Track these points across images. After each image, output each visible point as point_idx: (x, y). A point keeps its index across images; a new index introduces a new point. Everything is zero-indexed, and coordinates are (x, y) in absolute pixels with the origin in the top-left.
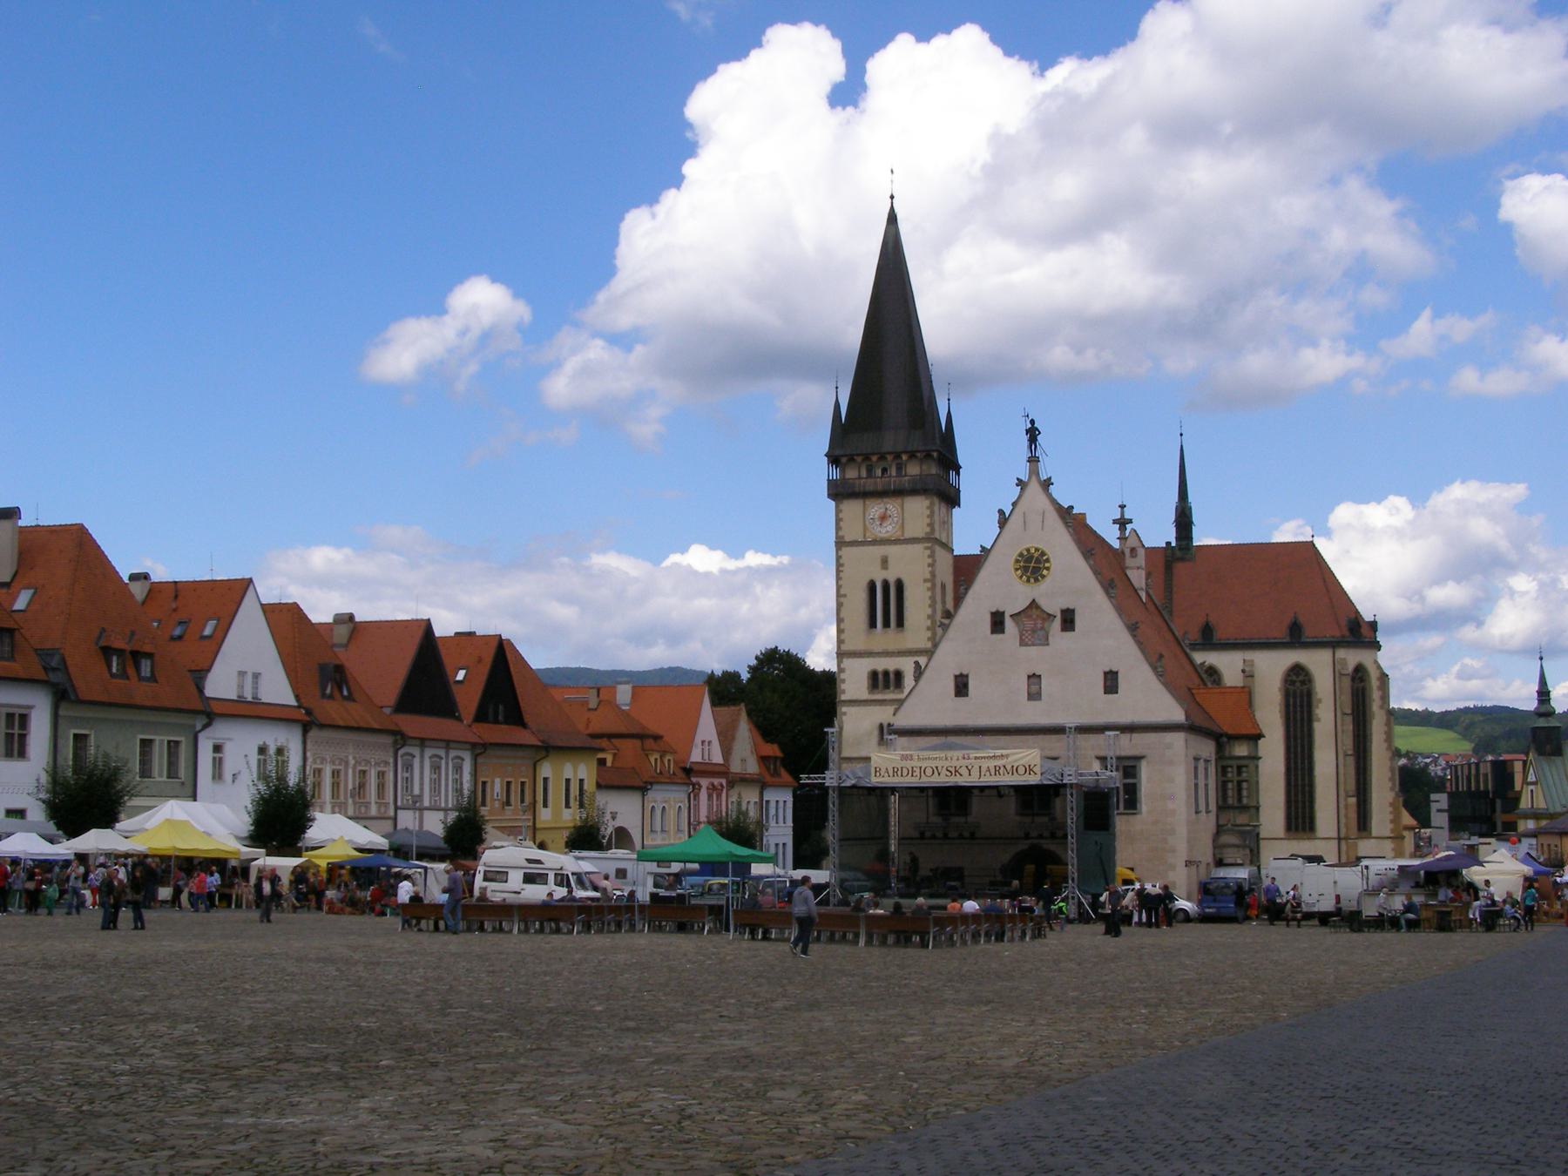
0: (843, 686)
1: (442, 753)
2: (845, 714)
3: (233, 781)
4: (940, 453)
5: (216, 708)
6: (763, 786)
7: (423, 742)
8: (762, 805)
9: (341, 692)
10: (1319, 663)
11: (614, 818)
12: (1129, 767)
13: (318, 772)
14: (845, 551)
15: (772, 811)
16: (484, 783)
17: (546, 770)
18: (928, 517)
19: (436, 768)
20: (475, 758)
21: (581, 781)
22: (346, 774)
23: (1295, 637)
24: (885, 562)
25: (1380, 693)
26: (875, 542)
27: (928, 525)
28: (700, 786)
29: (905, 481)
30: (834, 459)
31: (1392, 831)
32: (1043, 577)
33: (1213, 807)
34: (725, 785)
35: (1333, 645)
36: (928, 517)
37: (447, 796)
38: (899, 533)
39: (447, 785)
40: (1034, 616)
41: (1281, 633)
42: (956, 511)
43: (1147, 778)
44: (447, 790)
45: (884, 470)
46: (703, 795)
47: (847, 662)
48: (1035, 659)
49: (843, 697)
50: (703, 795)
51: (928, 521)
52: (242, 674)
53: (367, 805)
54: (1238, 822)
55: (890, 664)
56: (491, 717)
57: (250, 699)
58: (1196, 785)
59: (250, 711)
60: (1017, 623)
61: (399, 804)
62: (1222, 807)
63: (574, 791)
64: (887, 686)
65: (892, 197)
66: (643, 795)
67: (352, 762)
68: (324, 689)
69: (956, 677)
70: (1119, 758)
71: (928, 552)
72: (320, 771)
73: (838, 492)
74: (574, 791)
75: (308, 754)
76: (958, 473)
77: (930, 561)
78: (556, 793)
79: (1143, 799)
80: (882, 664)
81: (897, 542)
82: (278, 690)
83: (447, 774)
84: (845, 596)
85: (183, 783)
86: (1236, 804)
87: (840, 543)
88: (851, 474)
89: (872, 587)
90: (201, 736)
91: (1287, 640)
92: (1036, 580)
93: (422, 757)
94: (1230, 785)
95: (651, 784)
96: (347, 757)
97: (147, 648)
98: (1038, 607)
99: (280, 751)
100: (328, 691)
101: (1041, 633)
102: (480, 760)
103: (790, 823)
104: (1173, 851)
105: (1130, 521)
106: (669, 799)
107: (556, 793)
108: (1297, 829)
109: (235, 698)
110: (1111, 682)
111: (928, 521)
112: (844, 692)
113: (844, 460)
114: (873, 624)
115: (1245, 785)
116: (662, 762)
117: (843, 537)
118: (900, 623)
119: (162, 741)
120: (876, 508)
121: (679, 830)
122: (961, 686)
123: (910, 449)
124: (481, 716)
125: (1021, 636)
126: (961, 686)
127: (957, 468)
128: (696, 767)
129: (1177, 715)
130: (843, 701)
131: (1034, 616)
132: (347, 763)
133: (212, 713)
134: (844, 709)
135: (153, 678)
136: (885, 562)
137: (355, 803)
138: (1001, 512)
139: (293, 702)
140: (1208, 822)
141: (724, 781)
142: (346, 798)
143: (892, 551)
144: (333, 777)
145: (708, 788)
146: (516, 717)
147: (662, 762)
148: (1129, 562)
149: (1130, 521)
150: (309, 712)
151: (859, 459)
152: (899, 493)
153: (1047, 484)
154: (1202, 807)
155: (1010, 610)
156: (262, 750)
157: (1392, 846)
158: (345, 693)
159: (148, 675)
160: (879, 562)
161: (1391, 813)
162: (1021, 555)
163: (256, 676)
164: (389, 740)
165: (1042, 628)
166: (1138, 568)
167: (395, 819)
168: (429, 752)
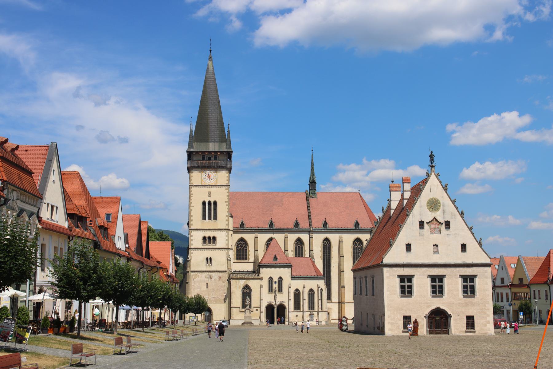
0: (192, 242)
2: (192, 253)
14: (193, 189)
18: (227, 177)
24: (209, 194)
26: (205, 186)
27: (227, 180)
36: (227, 177)
40: (435, 223)
41: (352, 226)
48: (436, 239)
51: (227, 178)
60: (429, 226)
64: (209, 242)
69: (406, 245)
71: (227, 191)
79: (477, 291)
81: (215, 186)
84: (193, 206)
89: (204, 203)
91: (354, 228)
98: (436, 220)
104: (489, 310)
110: (464, 248)
111: (227, 178)
112: (192, 245)
114: (204, 218)
118: (215, 218)
122: (408, 247)
123: (221, 150)
125: (430, 230)
126: (408, 247)
130: (192, 249)
131: (435, 223)
134: (192, 251)
136: (209, 194)
143: (212, 189)
151: (201, 153)
155: (426, 220)
160: (207, 194)
163: (121, 237)
165: (438, 228)
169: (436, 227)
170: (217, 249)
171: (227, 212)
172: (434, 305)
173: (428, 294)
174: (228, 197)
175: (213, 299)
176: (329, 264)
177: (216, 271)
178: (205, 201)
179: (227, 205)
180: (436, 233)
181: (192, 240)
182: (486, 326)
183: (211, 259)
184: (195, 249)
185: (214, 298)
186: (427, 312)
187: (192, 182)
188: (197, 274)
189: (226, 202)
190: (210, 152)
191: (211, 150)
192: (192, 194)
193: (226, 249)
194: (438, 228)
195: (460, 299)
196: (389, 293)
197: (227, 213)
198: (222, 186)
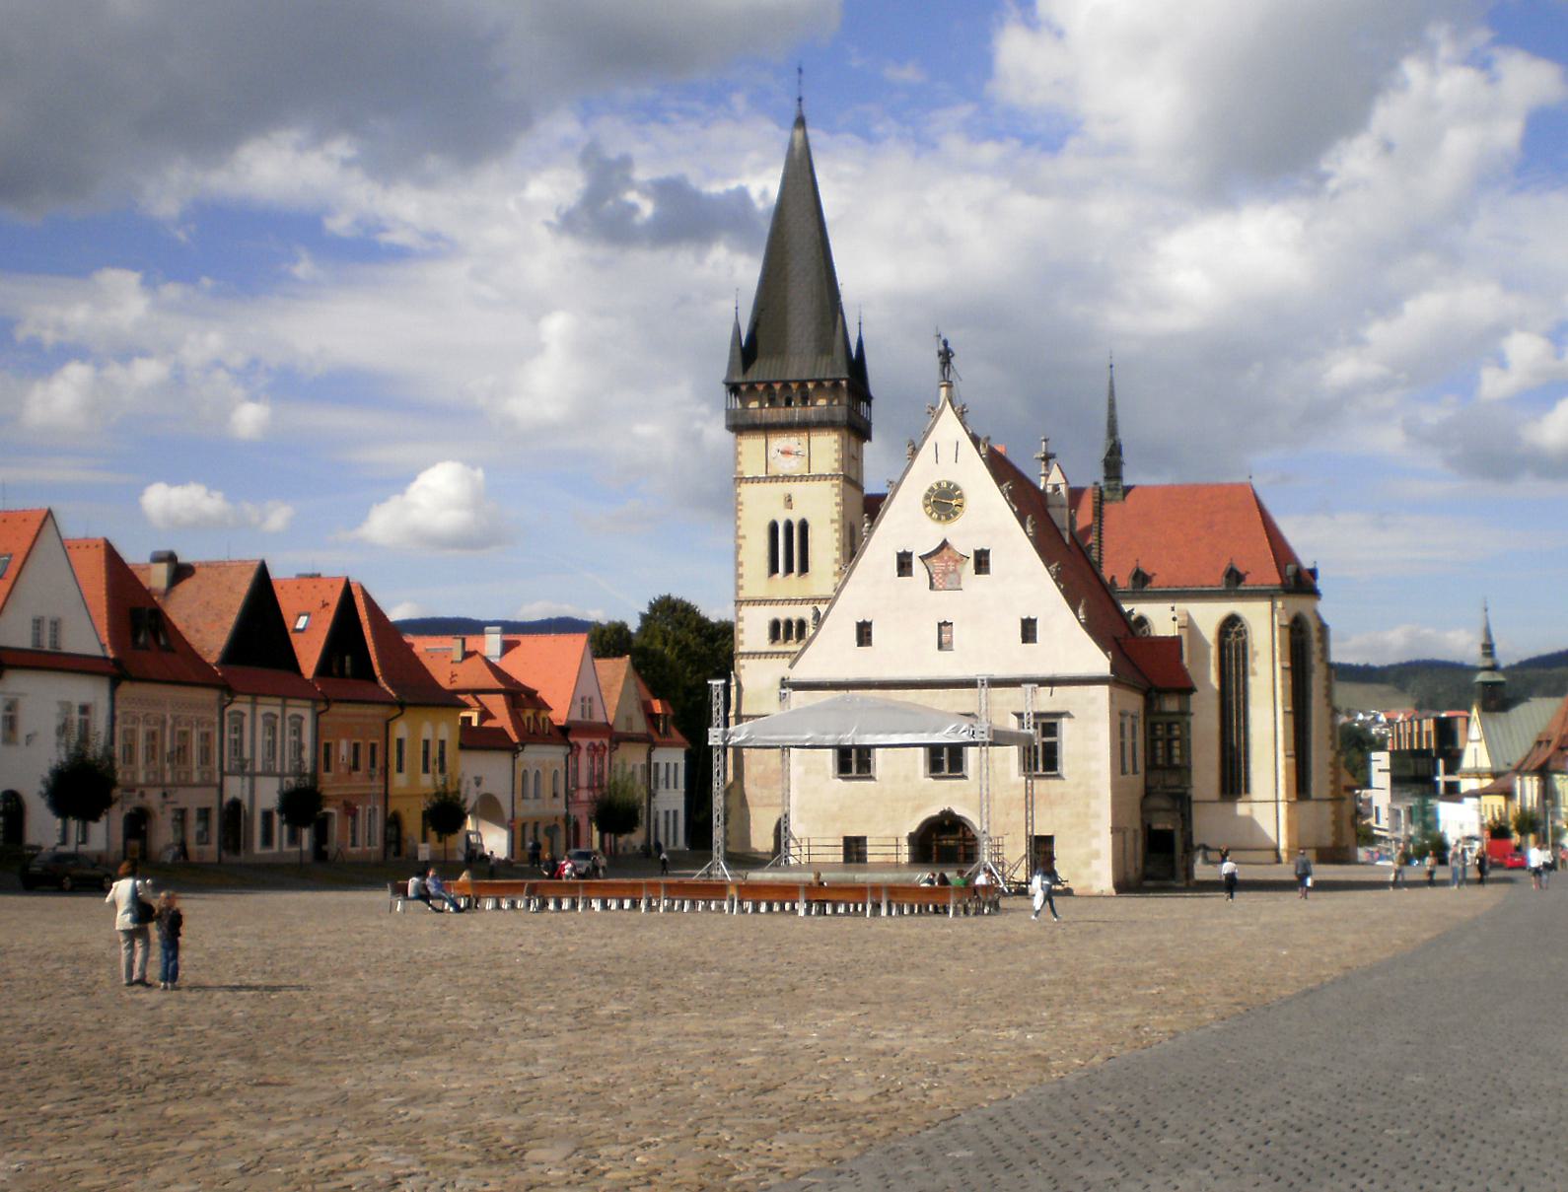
2: (743, 667)
8: (650, 769)
9: (157, 640)
11: (478, 783)
12: (1049, 724)
15: (662, 774)
16: (327, 746)
17: (400, 729)
20: (317, 716)
21: (442, 742)
26: (776, 478)
28: (579, 748)
30: (734, 389)
34: (607, 744)
42: (866, 445)
44: (283, 754)
46: (584, 759)
47: (745, 610)
48: (944, 604)
49: (741, 649)
50: (584, 759)
53: (189, 773)
55: (794, 613)
56: (335, 671)
58: (1122, 744)
61: (226, 769)
63: (434, 752)
67: (170, 722)
68: (135, 636)
70: (1037, 715)
71: (836, 490)
74: (434, 752)
76: (869, 404)
78: (413, 756)
80: (784, 613)
81: (802, 478)
83: (283, 736)
84: (744, 537)
89: (773, 528)
92: (948, 518)
95: (523, 745)
100: (142, 639)
101: (952, 576)
102: (324, 719)
103: (682, 788)
106: (545, 758)
107: (413, 756)
110: (1028, 630)
112: (742, 643)
113: (744, 388)
114: (774, 569)
116: (536, 719)
117: (742, 473)
118: (804, 568)
120: (779, 442)
121: (555, 795)
122: (864, 633)
123: (817, 377)
126: (864, 633)
129: (1099, 663)
130: (743, 654)
132: (164, 722)
134: (742, 662)
136: (789, 500)
137: (173, 768)
140: (1137, 782)
141: (606, 742)
142: (162, 761)
145: (588, 749)
147: (536, 719)
152: (804, 426)
155: (918, 551)
162: (931, 490)
166: (1062, 506)
167: (221, 788)
171: (837, 549)
179: (836, 531)
180: (949, 586)
181: (742, 631)
182: (1087, 864)
184: (749, 654)
187: (739, 469)
189: (832, 521)
190: (786, 385)
191: (792, 375)
192: (741, 504)
194: (955, 571)
196: (801, 769)
198: (822, 477)
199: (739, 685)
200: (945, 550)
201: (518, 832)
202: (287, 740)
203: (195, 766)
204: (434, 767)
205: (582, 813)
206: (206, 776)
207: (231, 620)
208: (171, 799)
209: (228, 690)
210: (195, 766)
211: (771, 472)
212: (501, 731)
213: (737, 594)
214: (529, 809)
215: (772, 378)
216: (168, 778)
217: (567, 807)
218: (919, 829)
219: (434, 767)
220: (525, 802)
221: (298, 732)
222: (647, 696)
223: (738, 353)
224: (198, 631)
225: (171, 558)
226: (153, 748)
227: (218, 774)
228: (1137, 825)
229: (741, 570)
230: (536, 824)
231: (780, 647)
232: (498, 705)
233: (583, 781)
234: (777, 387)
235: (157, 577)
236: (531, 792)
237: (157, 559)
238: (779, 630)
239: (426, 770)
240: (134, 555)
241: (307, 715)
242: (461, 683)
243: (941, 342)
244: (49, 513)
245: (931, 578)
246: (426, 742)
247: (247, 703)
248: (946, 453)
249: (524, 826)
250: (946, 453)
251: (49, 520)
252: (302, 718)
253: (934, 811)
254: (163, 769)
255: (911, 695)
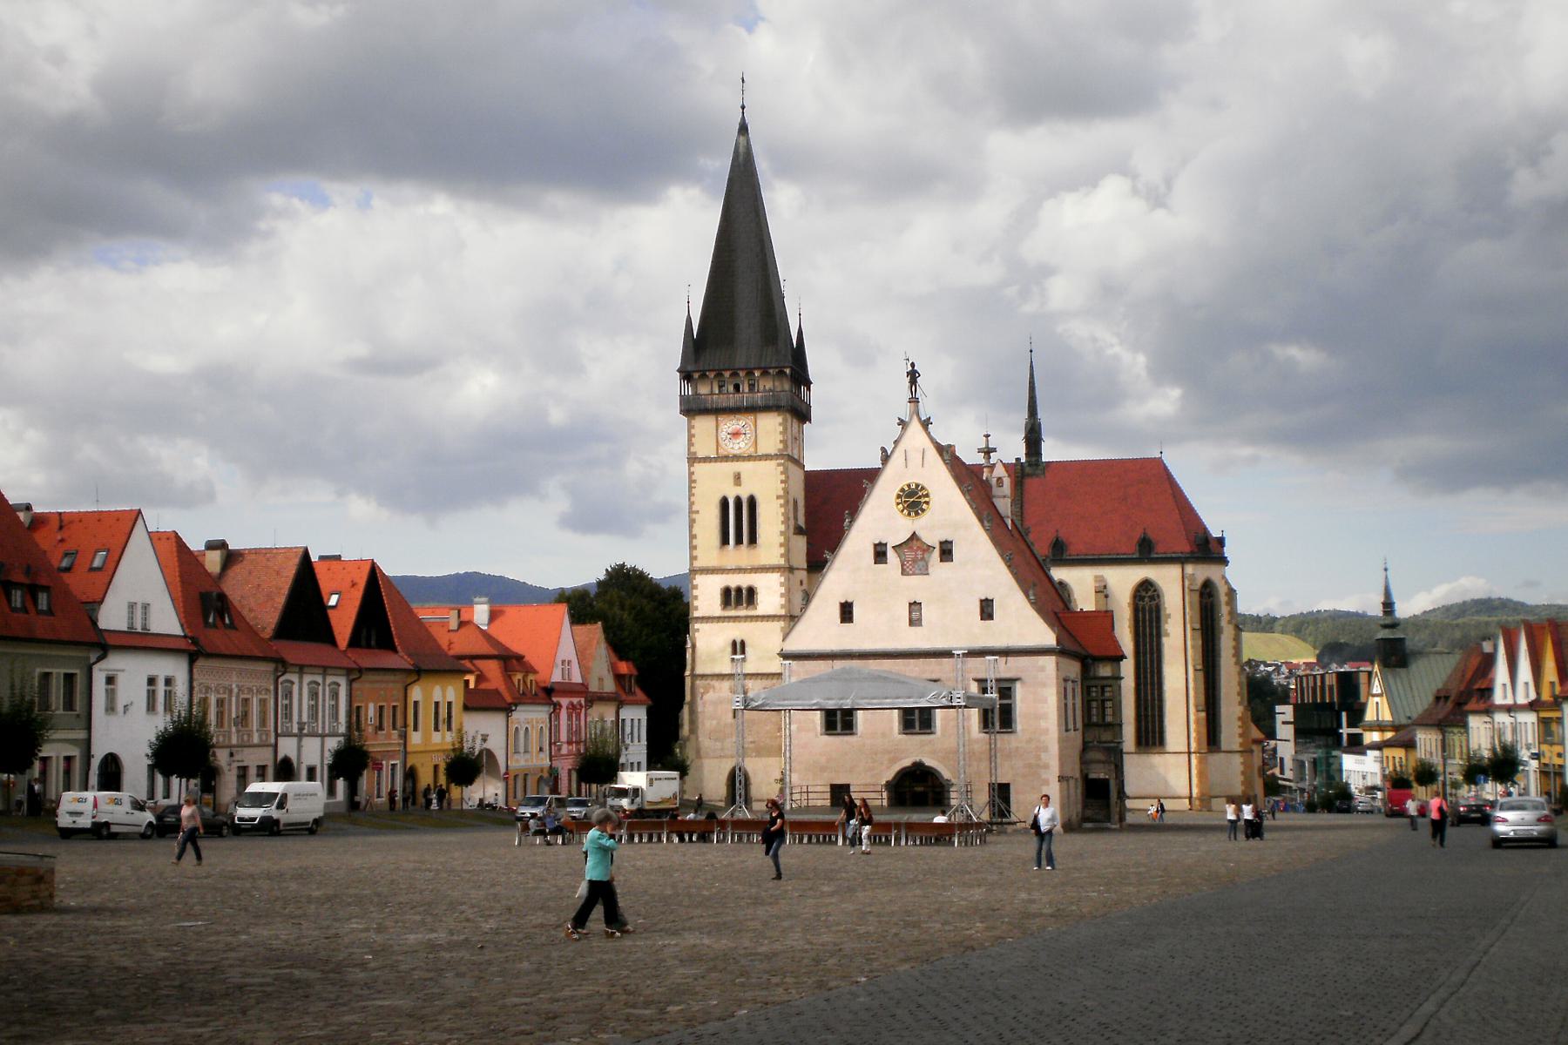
0: (696, 603)
1: (319, 679)
2: (698, 630)
3: (125, 713)
4: (792, 369)
5: (111, 641)
6: (620, 704)
7: (301, 669)
8: (618, 723)
9: (223, 620)
10: (1170, 581)
12: (1006, 688)
13: (204, 701)
14: (698, 467)
15: (628, 730)
16: (358, 708)
17: (416, 693)
18: (781, 433)
19: (314, 695)
20: (350, 683)
21: (450, 704)
22: (230, 700)
23: (1146, 553)
24: (737, 478)
25: (1229, 608)
26: (726, 458)
28: (561, 706)
29: (758, 398)
30: (686, 376)
31: (1241, 745)
32: (923, 510)
33: (1079, 725)
34: (583, 702)
35: (1181, 560)
36: (781, 433)
37: (324, 723)
38: (752, 450)
39: (324, 711)
41: (1131, 548)
42: (806, 426)
43: (1022, 699)
44: (324, 717)
45: (737, 388)
48: (915, 587)
49: (696, 614)
52: (132, 606)
53: (250, 735)
54: (1104, 739)
56: (363, 642)
57: (139, 630)
58: (1066, 705)
59: (140, 642)
61: (279, 731)
62: (1088, 725)
64: (739, 603)
65: (743, 107)
66: (508, 717)
67: (235, 690)
68: (206, 618)
70: (998, 680)
71: (781, 468)
72: (246, 701)
73: (692, 408)
75: (195, 684)
76: (809, 389)
77: (783, 477)
78: (427, 717)
79: (1018, 720)
80: (734, 581)
81: (749, 458)
82: (166, 620)
83: (324, 700)
84: (698, 512)
85: (78, 716)
86: (1100, 722)
87: (693, 459)
88: (704, 389)
89: (724, 503)
90: (96, 668)
92: (917, 514)
93: (301, 683)
94: (1094, 704)
95: (516, 705)
96: (231, 685)
97: (44, 582)
98: (918, 539)
99: (168, 681)
100: (211, 620)
101: (921, 563)
102: (355, 685)
103: (644, 742)
104: (1046, 767)
105: (994, 450)
106: (532, 717)
107: (427, 717)
108: (1147, 744)
109: (126, 629)
110: (987, 610)
112: (696, 609)
113: (696, 376)
114: (725, 541)
115: (1109, 704)
116: (525, 682)
117: (695, 453)
118: (753, 540)
119: (58, 674)
120: (729, 424)
121: (541, 749)
122: (846, 612)
123: (763, 365)
124: (355, 642)
126: (846, 612)
127: (808, 383)
128: (556, 687)
129: (1048, 637)
130: (697, 618)
132: (231, 691)
133: (105, 644)
134: (697, 626)
135: (50, 612)
136: (737, 478)
137: (238, 731)
138: (884, 450)
139: (178, 631)
140: (1076, 738)
141: (583, 701)
142: (230, 726)
143: (744, 467)
144: (218, 706)
145: (567, 708)
146: (387, 643)
147: (525, 682)
148: (996, 491)
149: (994, 450)
150: (195, 641)
151: (712, 375)
152: (752, 409)
153: (926, 424)
154: (1071, 726)
156: (151, 681)
157: (1241, 760)
158: (227, 621)
159: (45, 608)
160: (731, 480)
161: (1239, 727)
162: (902, 490)
163: (146, 607)
164: (270, 667)
166: (1005, 497)
167: (276, 746)
168: (307, 679)
169: (919, 557)
170: (758, 616)
172: (905, 758)
173: (892, 728)
174: (783, 485)
175: (752, 746)
176: (1207, 646)
177: (758, 675)
178: (728, 496)
181: (696, 598)
183: (743, 643)
185: (751, 742)
186: (889, 775)
187: (692, 449)
188: (709, 684)
189: (778, 497)
193: (780, 616)
194: (923, 559)
195: (977, 741)
197: (783, 526)
198: (767, 457)
199: (694, 647)
200: (915, 542)
201: (511, 782)
202: (327, 705)
203: (255, 728)
204: (443, 726)
205: (565, 766)
206: (264, 737)
207: (281, 600)
208: (237, 757)
209: (282, 665)
210: (255, 728)
211: (722, 452)
212: (497, 691)
213: (691, 564)
214: (520, 762)
215: (722, 367)
216: (234, 741)
217: (551, 760)
218: (895, 778)
219: (443, 726)
220: (516, 756)
221: (335, 695)
222: (615, 659)
223: (691, 344)
224: (251, 610)
225: (221, 545)
226: (222, 713)
227: (273, 734)
228: (1078, 775)
229: (695, 542)
230: (526, 775)
231: (733, 613)
232: (492, 669)
233: (564, 737)
234: (727, 374)
235: (213, 561)
236: (522, 749)
237: (211, 546)
238: (731, 597)
239: (436, 729)
240: (195, 544)
241: (343, 681)
242: (457, 649)
243: (909, 364)
244: (140, 510)
245: (903, 565)
246: (437, 704)
247: (319, 674)
248: (915, 458)
249: (516, 776)
250: (915, 458)
251: (140, 521)
252: (339, 685)
253: (907, 762)
254: (230, 732)
255: (887, 664)
